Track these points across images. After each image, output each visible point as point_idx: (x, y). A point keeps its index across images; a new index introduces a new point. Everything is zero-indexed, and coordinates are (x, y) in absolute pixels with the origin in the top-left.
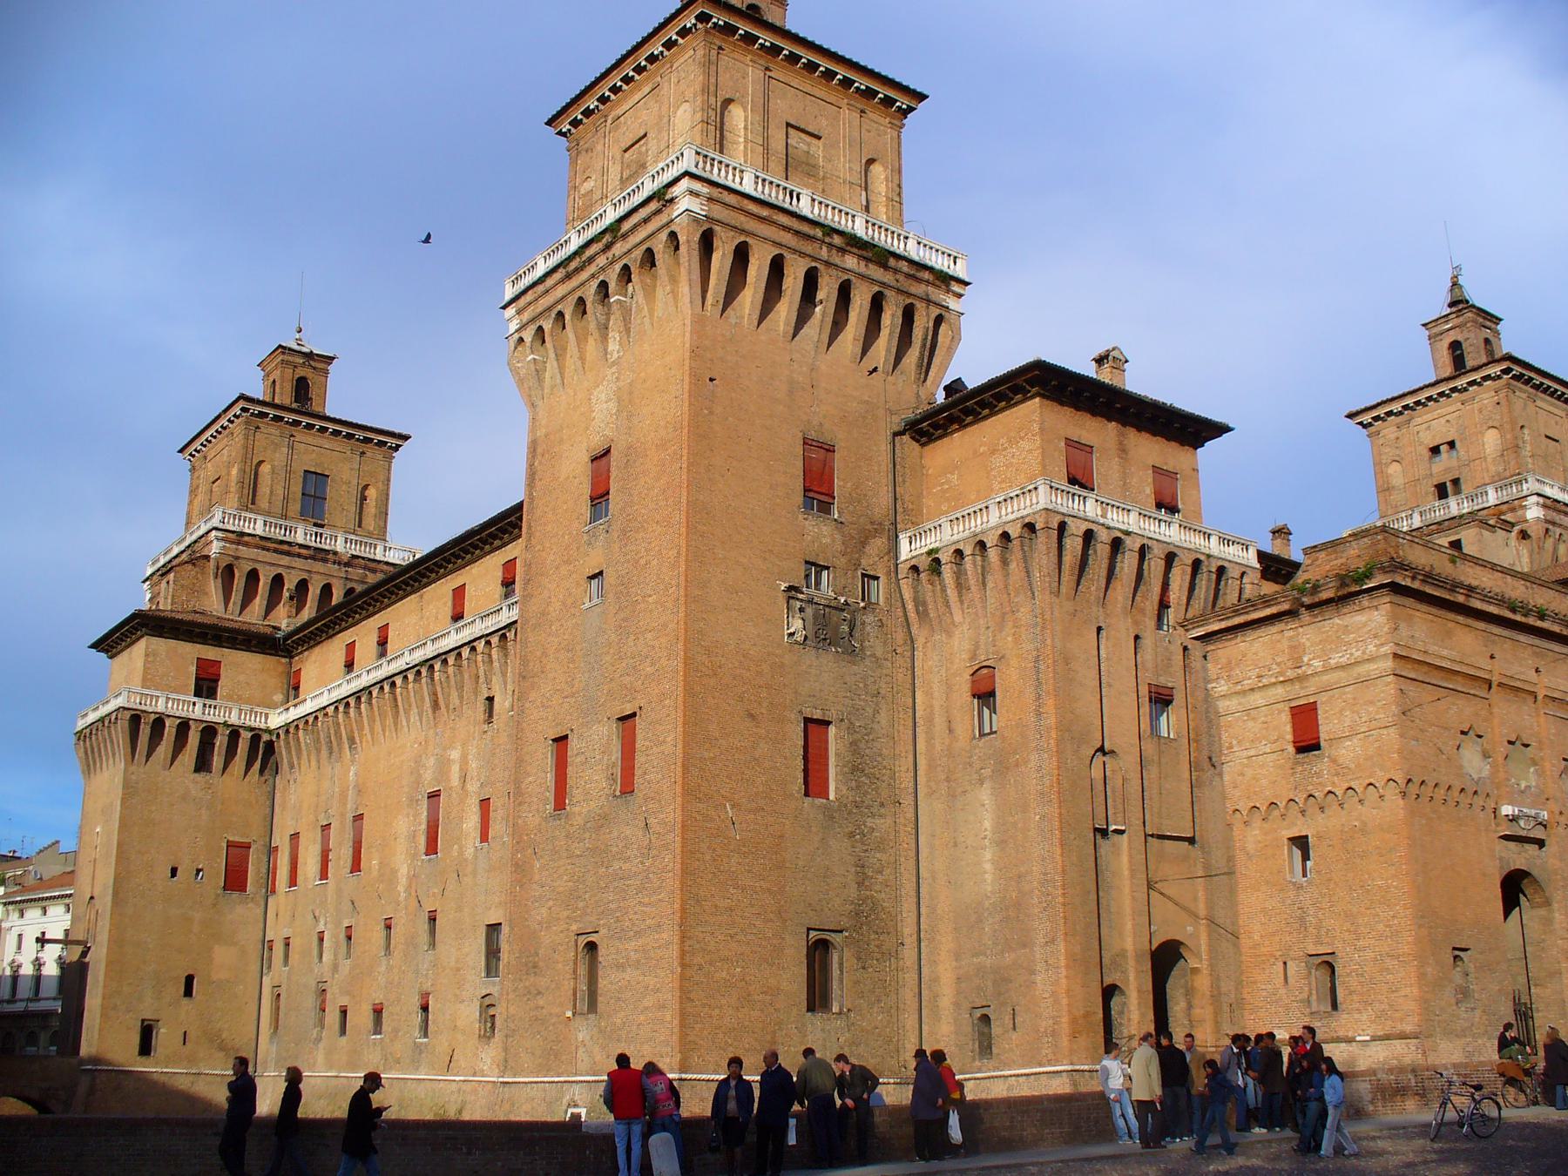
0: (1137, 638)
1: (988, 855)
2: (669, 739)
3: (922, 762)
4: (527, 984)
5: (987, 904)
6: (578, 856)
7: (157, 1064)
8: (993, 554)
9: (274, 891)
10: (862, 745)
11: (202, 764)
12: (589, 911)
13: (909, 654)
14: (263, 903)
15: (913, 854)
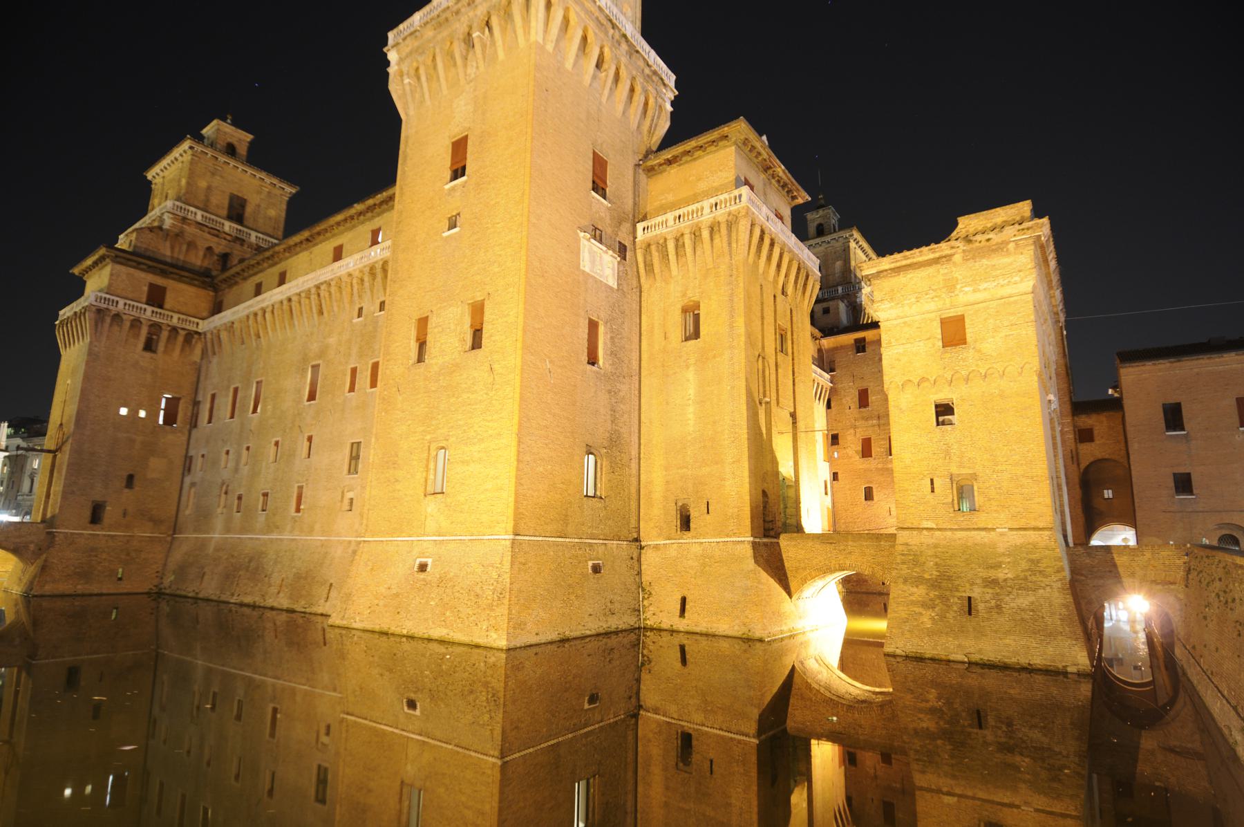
0: (775, 296)
1: (691, 409)
2: (511, 313)
3: (644, 356)
4: (387, 475)
5: (689, 438)
6: (433, 391)
7: (103, 529)
8: (706, 234)
9: (195, 426)
10: (616, 340)
11: (149, 346)
12: (441, 426)
13: (638, 293)
14: (187, 433)
15: (637, 408)
